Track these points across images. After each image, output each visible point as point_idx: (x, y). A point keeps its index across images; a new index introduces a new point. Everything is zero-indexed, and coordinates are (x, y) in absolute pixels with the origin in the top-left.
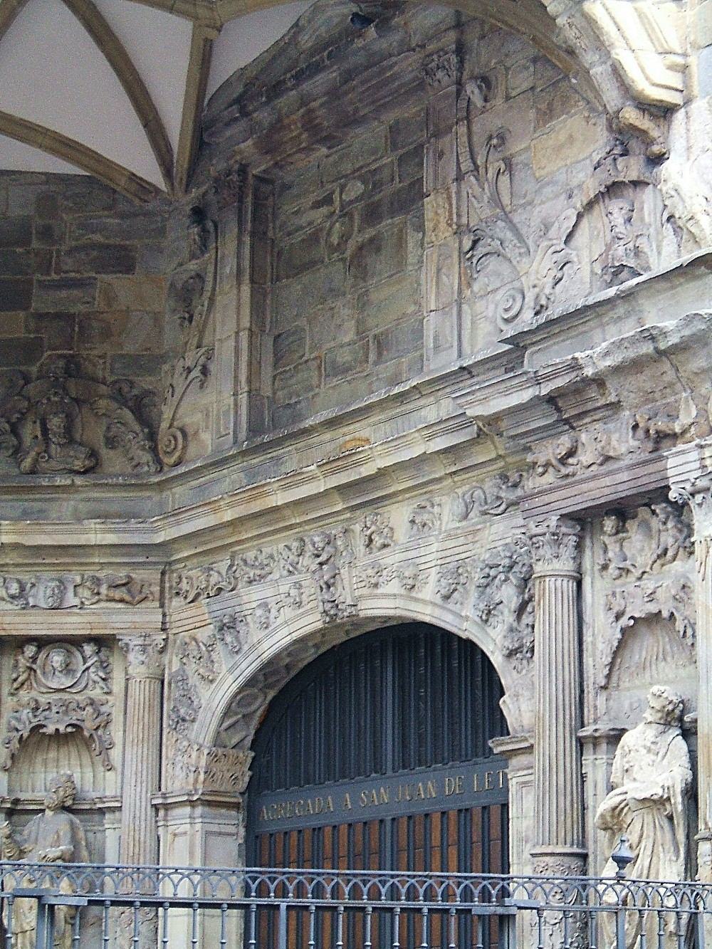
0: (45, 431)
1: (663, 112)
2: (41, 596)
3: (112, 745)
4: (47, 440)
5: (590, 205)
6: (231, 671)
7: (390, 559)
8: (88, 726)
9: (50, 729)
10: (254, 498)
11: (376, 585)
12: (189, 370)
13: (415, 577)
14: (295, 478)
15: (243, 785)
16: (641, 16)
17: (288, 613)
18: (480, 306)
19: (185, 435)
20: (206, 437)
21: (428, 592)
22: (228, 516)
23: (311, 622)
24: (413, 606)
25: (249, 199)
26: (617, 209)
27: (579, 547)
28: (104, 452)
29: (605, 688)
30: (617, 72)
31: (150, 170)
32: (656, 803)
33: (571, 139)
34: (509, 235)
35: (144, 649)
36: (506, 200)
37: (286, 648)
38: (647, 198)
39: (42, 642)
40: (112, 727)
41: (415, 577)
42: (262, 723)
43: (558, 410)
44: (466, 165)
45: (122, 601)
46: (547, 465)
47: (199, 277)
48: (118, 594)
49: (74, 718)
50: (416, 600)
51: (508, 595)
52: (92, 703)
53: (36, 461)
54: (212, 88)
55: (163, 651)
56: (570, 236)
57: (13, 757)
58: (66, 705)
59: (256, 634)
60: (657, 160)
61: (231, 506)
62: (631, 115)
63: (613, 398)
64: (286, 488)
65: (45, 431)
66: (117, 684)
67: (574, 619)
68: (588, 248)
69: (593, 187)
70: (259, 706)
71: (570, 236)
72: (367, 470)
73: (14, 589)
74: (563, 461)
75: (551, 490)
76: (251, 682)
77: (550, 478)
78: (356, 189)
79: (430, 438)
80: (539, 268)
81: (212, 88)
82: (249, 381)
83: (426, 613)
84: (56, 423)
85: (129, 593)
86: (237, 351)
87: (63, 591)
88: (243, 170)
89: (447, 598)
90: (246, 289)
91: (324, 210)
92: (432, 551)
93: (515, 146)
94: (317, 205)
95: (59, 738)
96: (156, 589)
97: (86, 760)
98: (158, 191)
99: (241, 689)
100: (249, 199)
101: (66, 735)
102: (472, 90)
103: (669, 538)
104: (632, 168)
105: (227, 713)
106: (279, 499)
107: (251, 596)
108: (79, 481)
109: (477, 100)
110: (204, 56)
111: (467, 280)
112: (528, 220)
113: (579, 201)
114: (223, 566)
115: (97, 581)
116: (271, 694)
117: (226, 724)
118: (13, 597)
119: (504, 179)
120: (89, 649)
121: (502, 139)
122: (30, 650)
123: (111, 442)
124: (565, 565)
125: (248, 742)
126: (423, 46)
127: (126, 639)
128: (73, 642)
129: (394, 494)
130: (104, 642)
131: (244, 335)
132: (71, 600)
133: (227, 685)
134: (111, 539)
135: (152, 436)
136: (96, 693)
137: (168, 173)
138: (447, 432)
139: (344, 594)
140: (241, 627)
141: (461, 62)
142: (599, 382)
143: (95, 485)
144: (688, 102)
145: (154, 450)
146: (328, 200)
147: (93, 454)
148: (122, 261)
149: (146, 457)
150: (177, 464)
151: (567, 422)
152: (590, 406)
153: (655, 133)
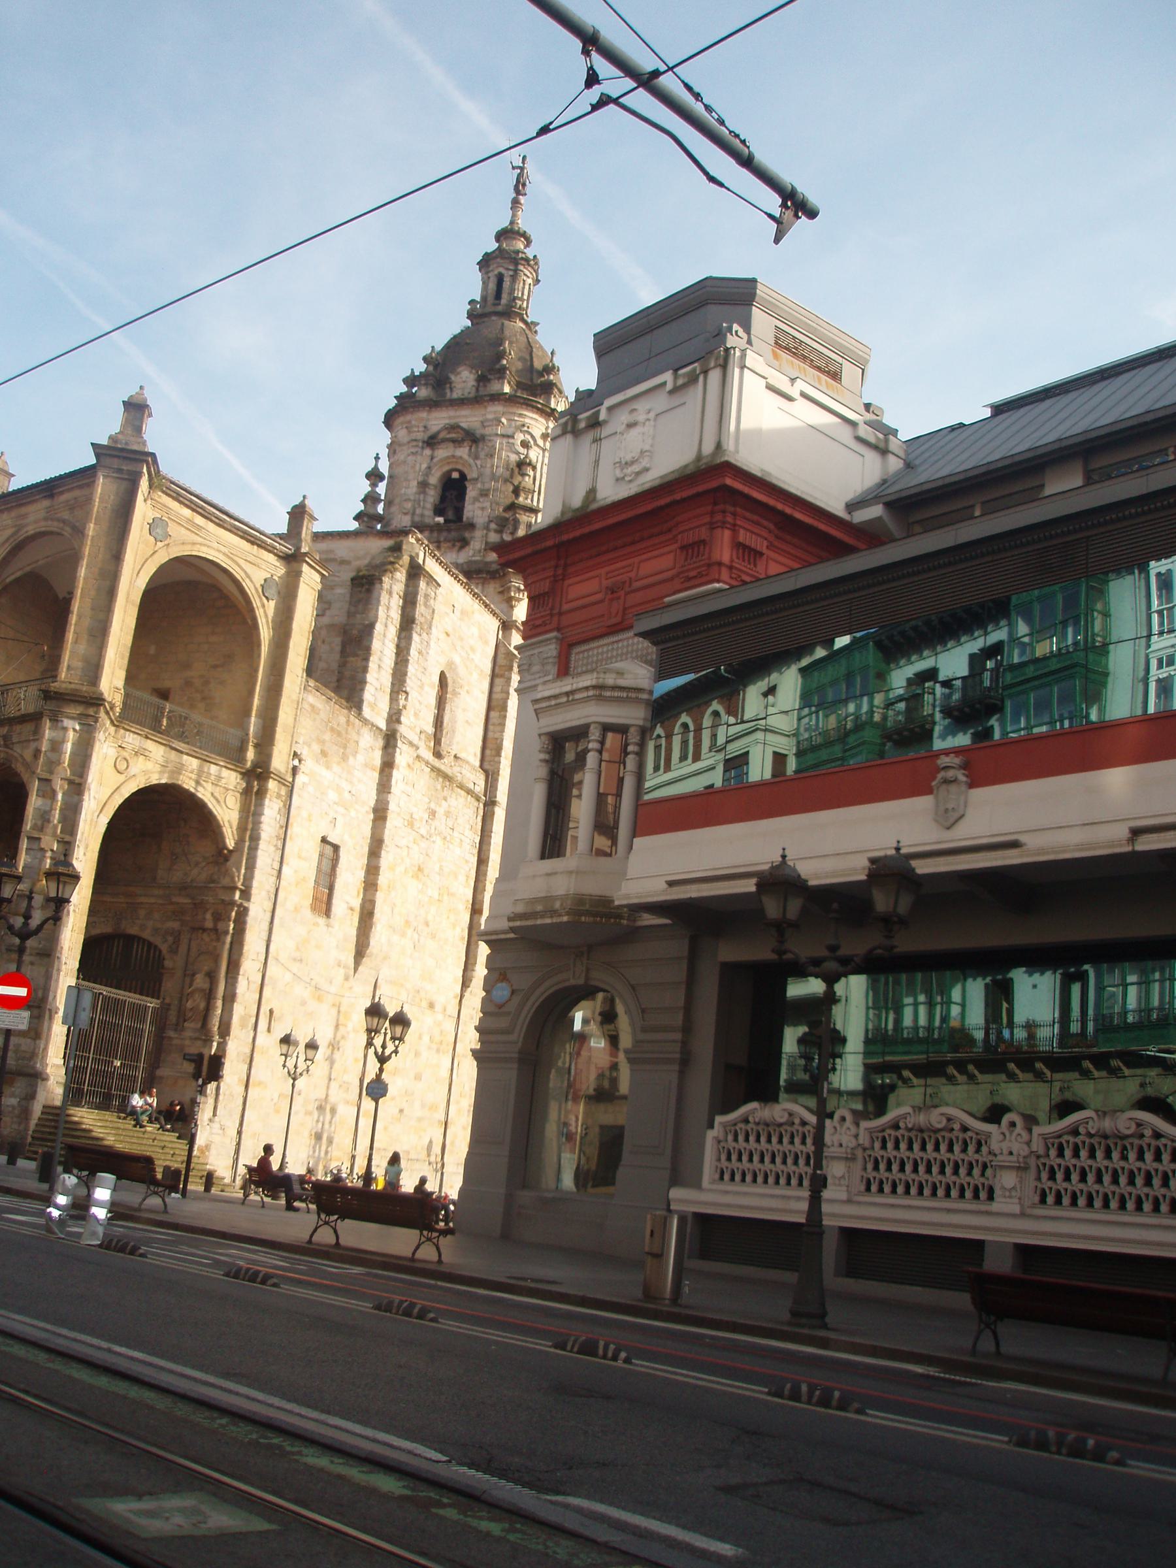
32: (203, 990)
51: (170, 939)
80: (195, 871)
103: (214, 937)
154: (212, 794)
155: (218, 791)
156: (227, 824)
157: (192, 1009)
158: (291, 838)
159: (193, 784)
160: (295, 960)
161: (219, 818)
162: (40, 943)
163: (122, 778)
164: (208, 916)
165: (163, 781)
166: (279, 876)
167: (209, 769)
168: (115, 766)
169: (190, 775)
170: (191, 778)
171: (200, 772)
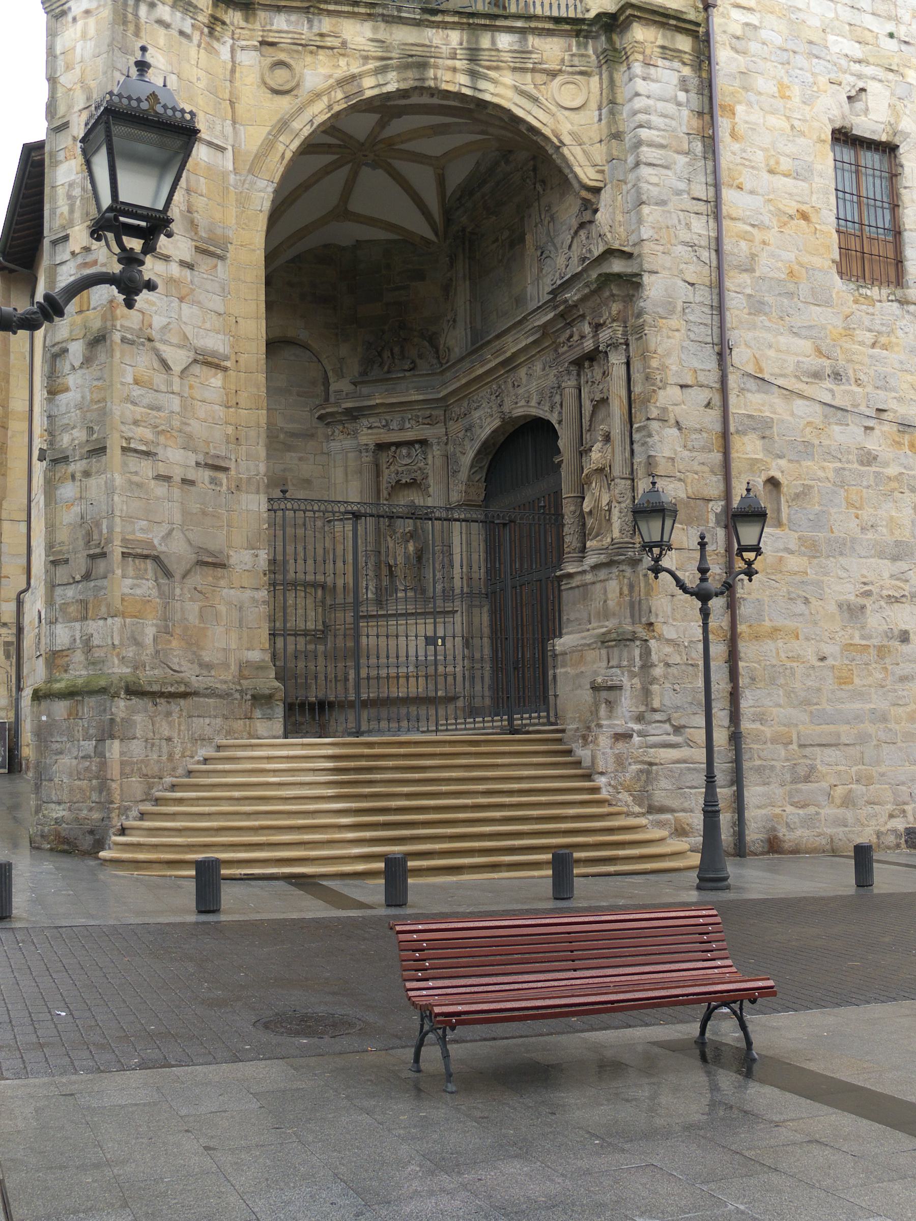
0: (392, 354)
1: (597, 191)
2: (394, 425)
3: (429, 486)
4: (393, 358)
5: (576, 233)
6: (471, 448)
7: (521, 391)
8: (419, 479)
9: (404, 481)
10: (472, 372)
11: (516, 403)
12: (449, 321)
13: (529, 397)
14: (484, 362)
15: (482, 497)
16: (584, 151)
17: (489, 420)
18: (545, 280)
19: (449, 350)
20: (457, 350)
21: (533, 403)
22: (464, 381)
23: (497, 423)
24: (530, 409)
25: (467, 243)
26: (583, 234)
27: (579, 375)
28: (418, 361)
29: (589, 430)
30: (576, 176)
31: (430, 235)
33: (570, 205)
34: (552, 248)
35: (438, 443)
36: (552, 234)
37: (490, 435)
38: (593, 227)
39: (398, 445)
40: (429, 479)
41: (529, 397)
42: (488, 470)
43: (565, 319)
44: (538, 220)
45: (428, 424)
46: (564, 343)
47: (451, 279)
48: (426, 421)
49: (413, 476)
50: (530, 407)
52: (420, 469)
53: (389, 367)
54: (449, 193)
55: (446, 444)
56: (570, 247)
57: (389, 494)
58: (409, 471)
59: (479, 431)
60: (596, 211)
61: (464, 377)
62: (584, 194)
63: (581, 312)
64: (482, 366)
65: (392, 354)
66: (430, 461)
67: (577, 404)
68: (575, 253)
69: (575, 226)
70: (486, 463)
71: (570, 247)
72: (508, 354)
73: (384, 423)
74: (568, 340)
75: (566, 352)
76: (479, 452)
77: (565, 348)
78: (506, 233)
79: (527, 337)
80: (561, 261)
81: (449, 193)
82: (471, 323)
83: (534, 412)
84: (397, 350)
85: (431, 421)
86: (465, 310)
87: (404, 422)
88: (464, 230)
89: (539, 404)
90: (467, 283)
91: (495, 245)
92: (533, 386)
93: (554, 210)
94: (494, 242)
95: (407, 485)
96: (442, 418)
97: (420, 493)
98: (434, 242)
99: (476, 455)
100: (467, 243)
101: (411, 484)
102: (539, 187)
104: (587, 216)
105: (472, 466)
106: (480, 371)
107: (476, 414)
108: (407, 374)
109: (541, 192)
110: (441, 181)
111: (541, 270)
112: (557, 241)
113: (572, 232)
114: (465, 404)
115: (418, 416)
116: (490, 457)
117: (473, 471)
118: (384, 426)
119: (551, 224)
120: (417, 446)
121: (549, 207)
122: (393, 449)
123: (421, 356)
124: (572, 382)
125: (483, 479)
126: (521, 168)
127: (431, 440)
128: (410, 444)
129: (519, 365)
130: (423, 443)
131: (468, 303)
132: (407, 425)
133: (471, 454)
134: (421, 397)
135: (437, 352)
136: (421, 465)
137: (436, 234)
138: (532, 334)
139: (506, 409)
140: (473, 429)
141: (535, 174)
142: (575, 306)
143: (414, 375)
144: (605, 186)
145: (438, 358)
146: (497, 240)
147: (413, 362)
148: (420, 276)
149: (435, 361)
150: (447, 363)
151: (569, 324)
152: (575, 316)
153: (593, 200)
154: (516, 87)
155: (527, 82)
156: (567, 139)
157: (591, 511)
158: (733, 135)
159: (463, 79)
160: (817, 375)
161: (547, 131)
162: (90, 430)
163: (285, 104)
164: (587, 329)
165: (391, 87)
166: (717, 214)
167: (493, 42)
168: (265, 83)
169: (450, 63)
170: (454, 70)
171: (473, 54)
